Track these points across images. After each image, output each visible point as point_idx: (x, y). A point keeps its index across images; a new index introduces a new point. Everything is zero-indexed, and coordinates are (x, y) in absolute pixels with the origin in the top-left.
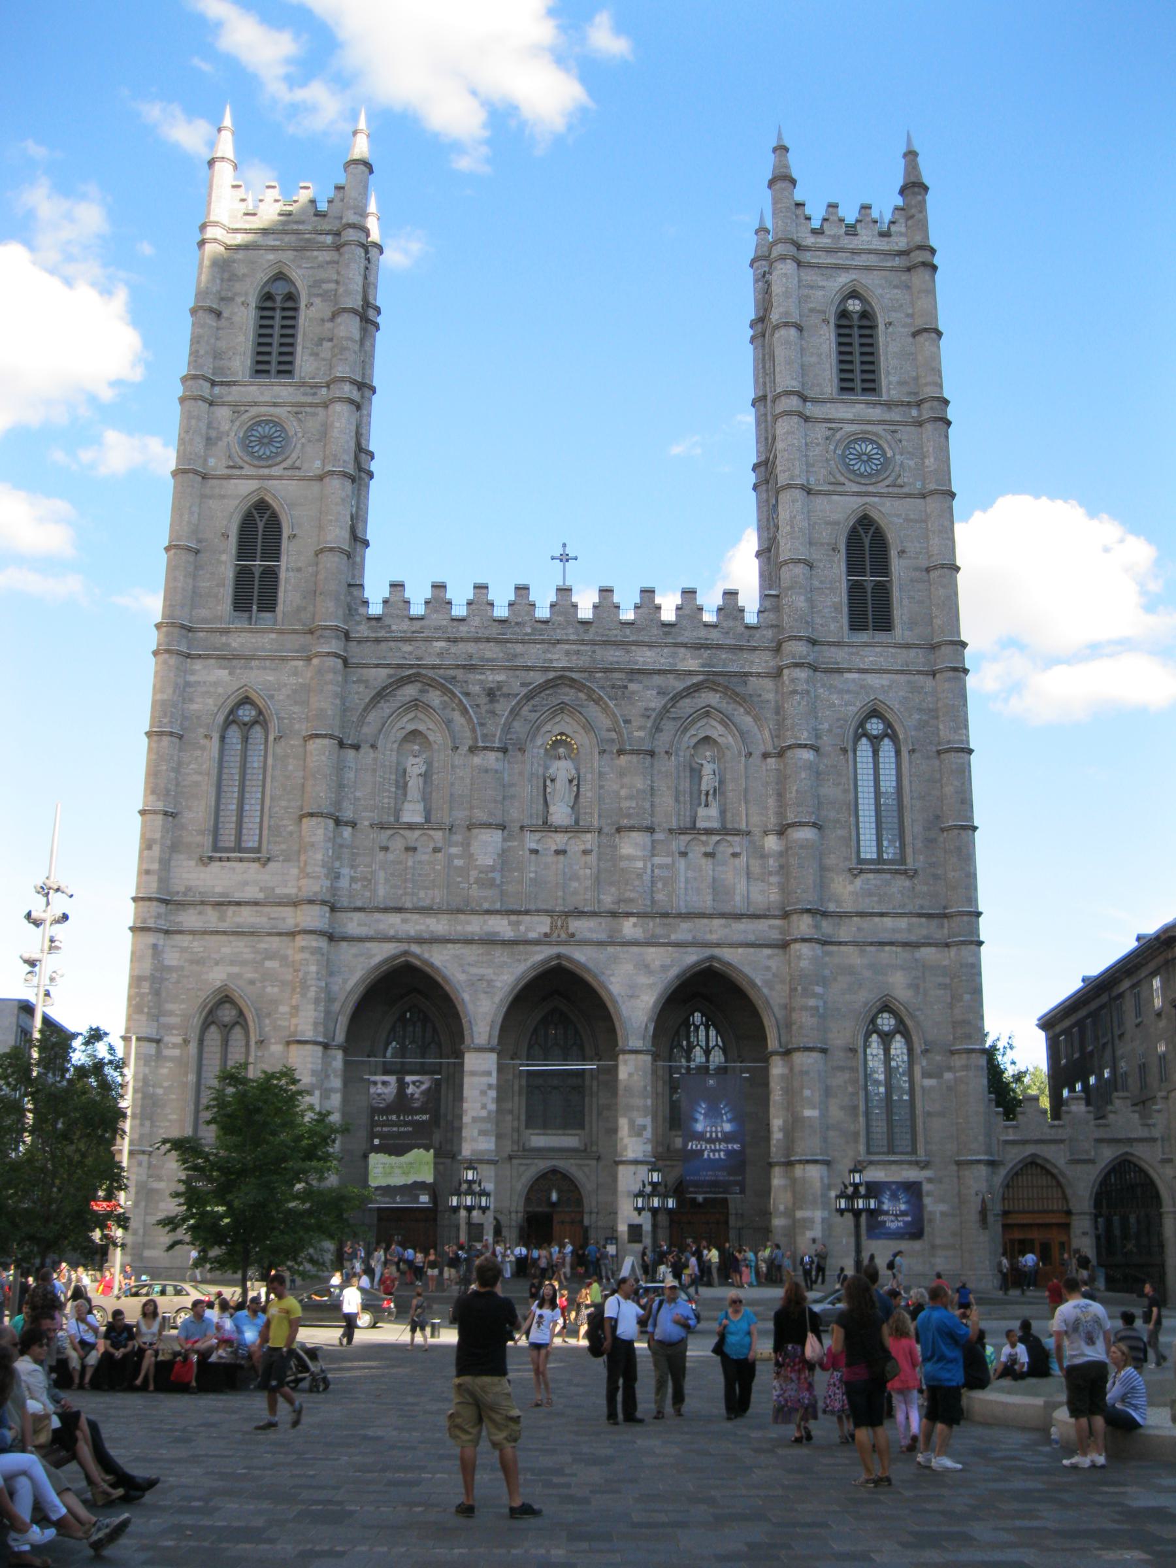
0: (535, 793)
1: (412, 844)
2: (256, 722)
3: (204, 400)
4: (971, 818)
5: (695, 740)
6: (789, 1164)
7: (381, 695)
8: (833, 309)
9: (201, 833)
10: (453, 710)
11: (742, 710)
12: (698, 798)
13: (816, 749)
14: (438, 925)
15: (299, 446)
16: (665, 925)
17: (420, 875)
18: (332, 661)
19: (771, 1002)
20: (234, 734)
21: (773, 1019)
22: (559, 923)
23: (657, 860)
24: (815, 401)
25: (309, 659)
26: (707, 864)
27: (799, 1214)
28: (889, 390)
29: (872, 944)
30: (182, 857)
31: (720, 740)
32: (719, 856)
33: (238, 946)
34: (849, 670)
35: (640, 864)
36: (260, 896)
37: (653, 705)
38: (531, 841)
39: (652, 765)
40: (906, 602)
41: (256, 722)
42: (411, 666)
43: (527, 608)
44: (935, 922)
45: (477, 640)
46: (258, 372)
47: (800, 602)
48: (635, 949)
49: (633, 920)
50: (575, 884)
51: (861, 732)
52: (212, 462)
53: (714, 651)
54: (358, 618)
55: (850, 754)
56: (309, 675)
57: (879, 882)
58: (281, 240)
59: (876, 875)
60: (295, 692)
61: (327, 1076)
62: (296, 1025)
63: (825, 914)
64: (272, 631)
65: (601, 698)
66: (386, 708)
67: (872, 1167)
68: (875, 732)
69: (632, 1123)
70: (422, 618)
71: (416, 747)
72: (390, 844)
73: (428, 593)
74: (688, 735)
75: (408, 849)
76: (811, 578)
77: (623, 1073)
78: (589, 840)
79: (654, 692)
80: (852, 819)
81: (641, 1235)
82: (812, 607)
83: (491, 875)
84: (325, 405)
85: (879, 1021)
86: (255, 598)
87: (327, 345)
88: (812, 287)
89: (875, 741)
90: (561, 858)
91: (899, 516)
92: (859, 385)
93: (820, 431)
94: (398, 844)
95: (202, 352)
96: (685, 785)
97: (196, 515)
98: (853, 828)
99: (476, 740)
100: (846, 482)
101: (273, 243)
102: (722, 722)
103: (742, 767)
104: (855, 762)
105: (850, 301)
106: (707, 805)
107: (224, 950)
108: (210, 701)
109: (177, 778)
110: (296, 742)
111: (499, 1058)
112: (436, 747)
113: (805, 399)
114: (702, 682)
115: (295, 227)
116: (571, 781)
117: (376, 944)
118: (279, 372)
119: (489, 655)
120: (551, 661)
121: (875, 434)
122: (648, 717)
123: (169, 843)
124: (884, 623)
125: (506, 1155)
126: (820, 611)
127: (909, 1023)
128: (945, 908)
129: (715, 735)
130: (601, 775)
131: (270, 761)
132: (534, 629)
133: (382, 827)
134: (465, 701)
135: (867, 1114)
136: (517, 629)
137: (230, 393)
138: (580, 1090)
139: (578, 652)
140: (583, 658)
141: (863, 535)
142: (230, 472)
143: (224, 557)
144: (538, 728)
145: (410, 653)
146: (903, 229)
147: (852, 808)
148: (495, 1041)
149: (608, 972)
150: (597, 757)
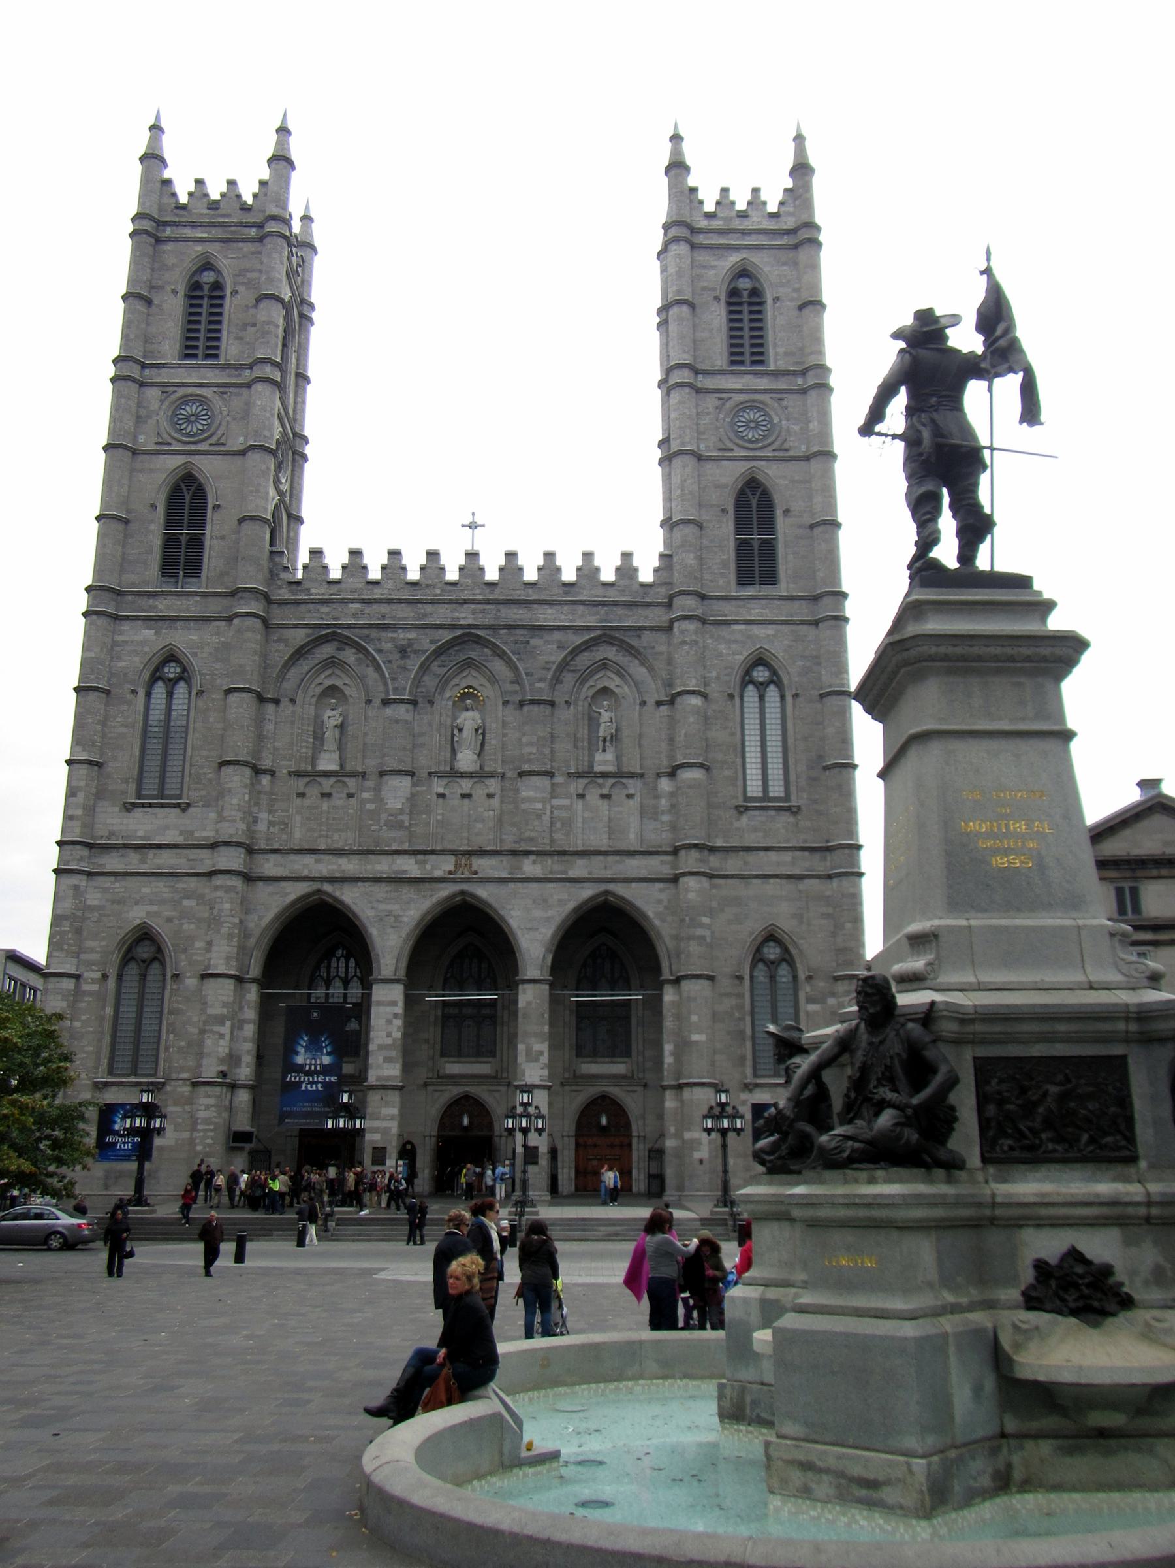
0: (443, 742)
1: (327, 790)
2: (180, 678)
3: (133, 380)
4: (851, 757)
5: (593, 691)
6: (680, 1087)
7: (300, 653)
8: (724, 287)
9: (126, 781)
10: (367, 666)
11: (637, 662)
12: (595, 743)
13: (704, 696)
14: (349, 866)
15: (224, 423)
17: (334, 819)
18: (251, 621)
19: (664, 933)
20: (160, 689)
22: (463, 862)
23: (555, 802)
24: (705, 373)
25: (230, 619)
26: (604, 806)
27: (687, 1135)
28: (776, 361)
29: (757, 877)
30: (106, 803)
31: (617, 690)
32: (614, 797)
33: (160, 885)
34: (736, 622)
35: (539, 806)
36: (180, 840)
37: (552, 658)
38: (438, 786)
39: (552, 714)
40: (791, 557)
41: (180, 678)
42: (328, 626)
43: (437, 571)
44: (818, 855)
45: (390, 601)
46: (187, 356)
47: (690, 559)
48: (534, 885)
49: (533, 857)
50: (479, 826)
51: (747, 679)
52: (141, 438)
53: (611, 607)
54: (279, 583)
55: (737, 699)
56: (231, 634)
57: (764, 819)
58: (209, 233)
59: (762, 812)
60: (217, 650)
61: (241, 1008)
62: (210, 959)
63: (712, 850)
64: (196, 594)
65: (504, 652)
66: (304, 666)
67: (758, 1090)
68: (761, 679)
69: (529, 1051)
70: (337, 582)
71: (333, 701)
72: (307, 791)
73: (345, 559)
74: (587, 685)
75: (323, 795)
76: (701, 537)
77: (522, 1004)
78: (493, 785)
79: (555, 647)
80: (739, 760)
81: (537, 1157)
82: (702, 565)
83: (400, 817)
84: (248, 386)
85: (765, 950)
86: (182, 565)
87: (251, 330)
88: (704, 267)
89: (761, 687)
90: (466, 801)
91: (784, 477)
92: (747, 358)
93: (711, 402)
94: (313, 792)
95: (132, 336)
96: (583, 733)
97: (126, 488)
98: (740, 768)
99: (387, 693)
100: (735, 447)
101: (200, 235)
102: (618, 673)
103: (637, 714)
104: (742, 707)
105: (741, 280)
106: (604, 751)
107: (146, 890)
108: (137, 659)
109: (103, 730)
110: (218, 696)
111: (407, 988)
112: (351, 700)
113: (697, 372)
114: (600, 637)
115: (222, 220)
116: (477, 730)
117: (291, 883)
118: (208, 356)
119: (400, 614)
120: (458, 619)
121: (761, 402)
122: (549, 669)
123: (94, 790)
124: (770, 578)
125: (421, 1082)
126: (709, 568)
127: (793, 951)
128: (828, 841)
130: (504, 724)
131: (192, 714)
132: (442, 590)
133: (299, 774)
134: (378, 658)
135: (753, 1038)
136: (428, 591)
137: (159, 375)
138: (493, 1019)
139: (483, 611)
140: (489, 616)
141: (751, 497)
142: (158, 448)
143: (152, 527)
144: (447, 682)
145: (328, 614)
146: (791, 210)
147: (739, 749)
148: (402, 973)
149: (509, 907)
150: (500, 707)
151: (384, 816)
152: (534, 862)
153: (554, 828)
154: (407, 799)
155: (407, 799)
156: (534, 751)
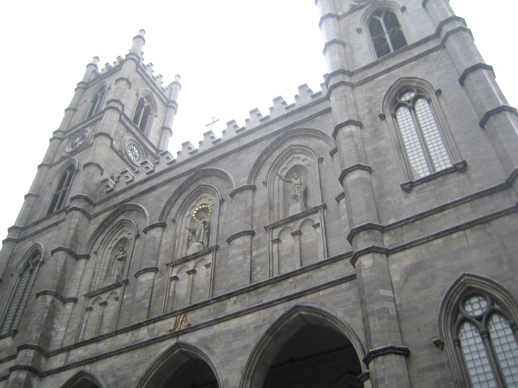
16: (257, 294)
21: (358, 344)
31: (304, 164)
49: (233, 299)
55: (389, 118)
63: (383, 230)
89: (411, 106)
129: (299, 162)
152: (235, 302)
153: (254, 273)
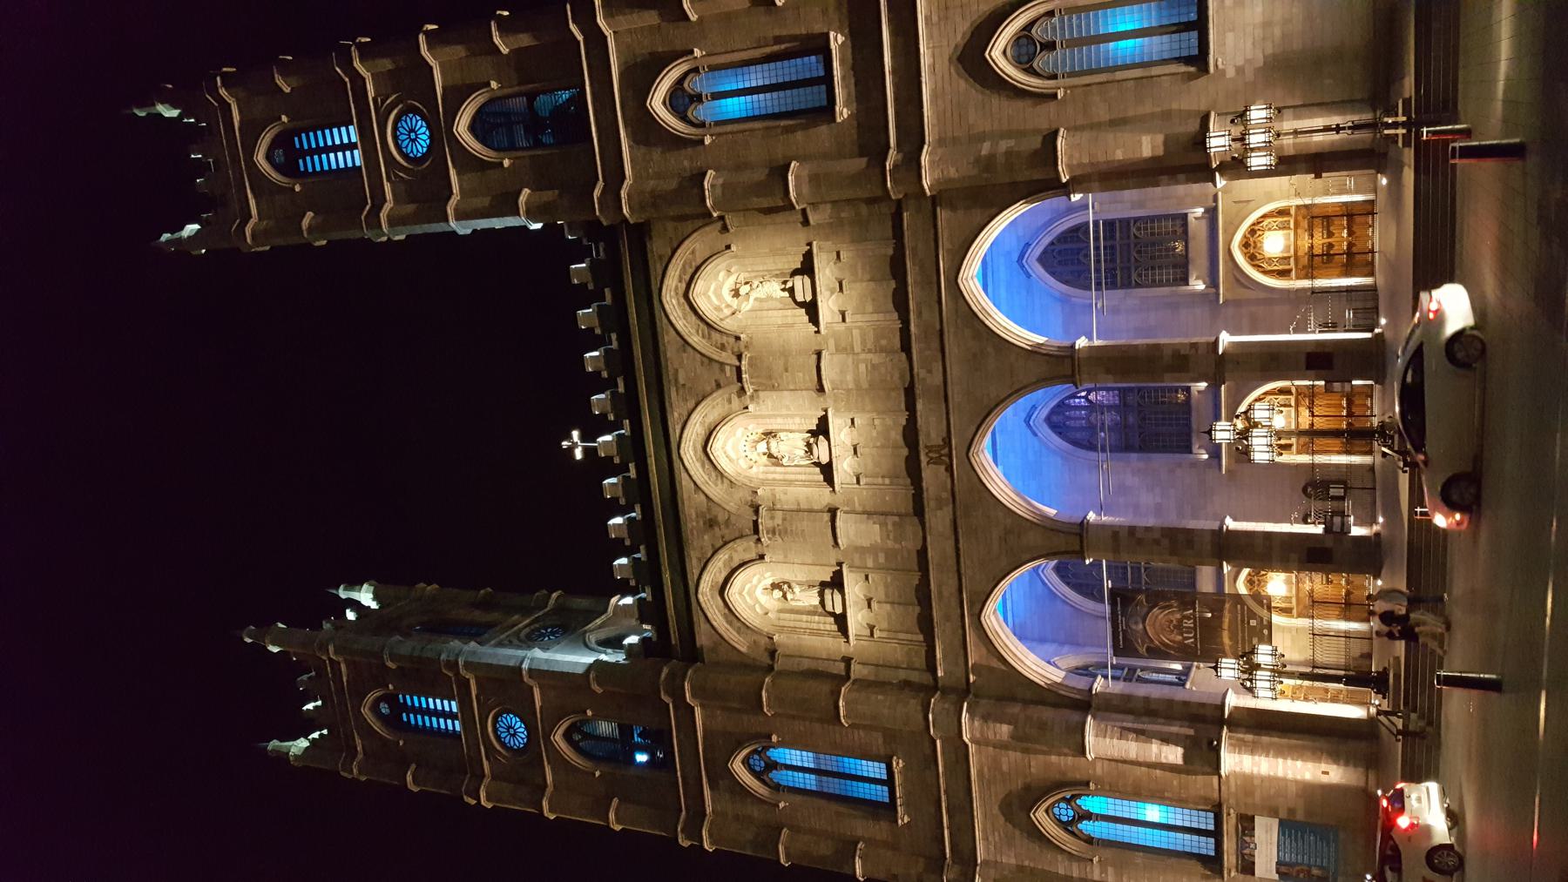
17: (900, 596)
35: (862, 367)
48: (954, 371)
79: (685, 355)
83: (890, 527)
106: (791, 291)
151: (890, 544)
154: (868, 518)
155: (868, 518)
156: (801, 375)
